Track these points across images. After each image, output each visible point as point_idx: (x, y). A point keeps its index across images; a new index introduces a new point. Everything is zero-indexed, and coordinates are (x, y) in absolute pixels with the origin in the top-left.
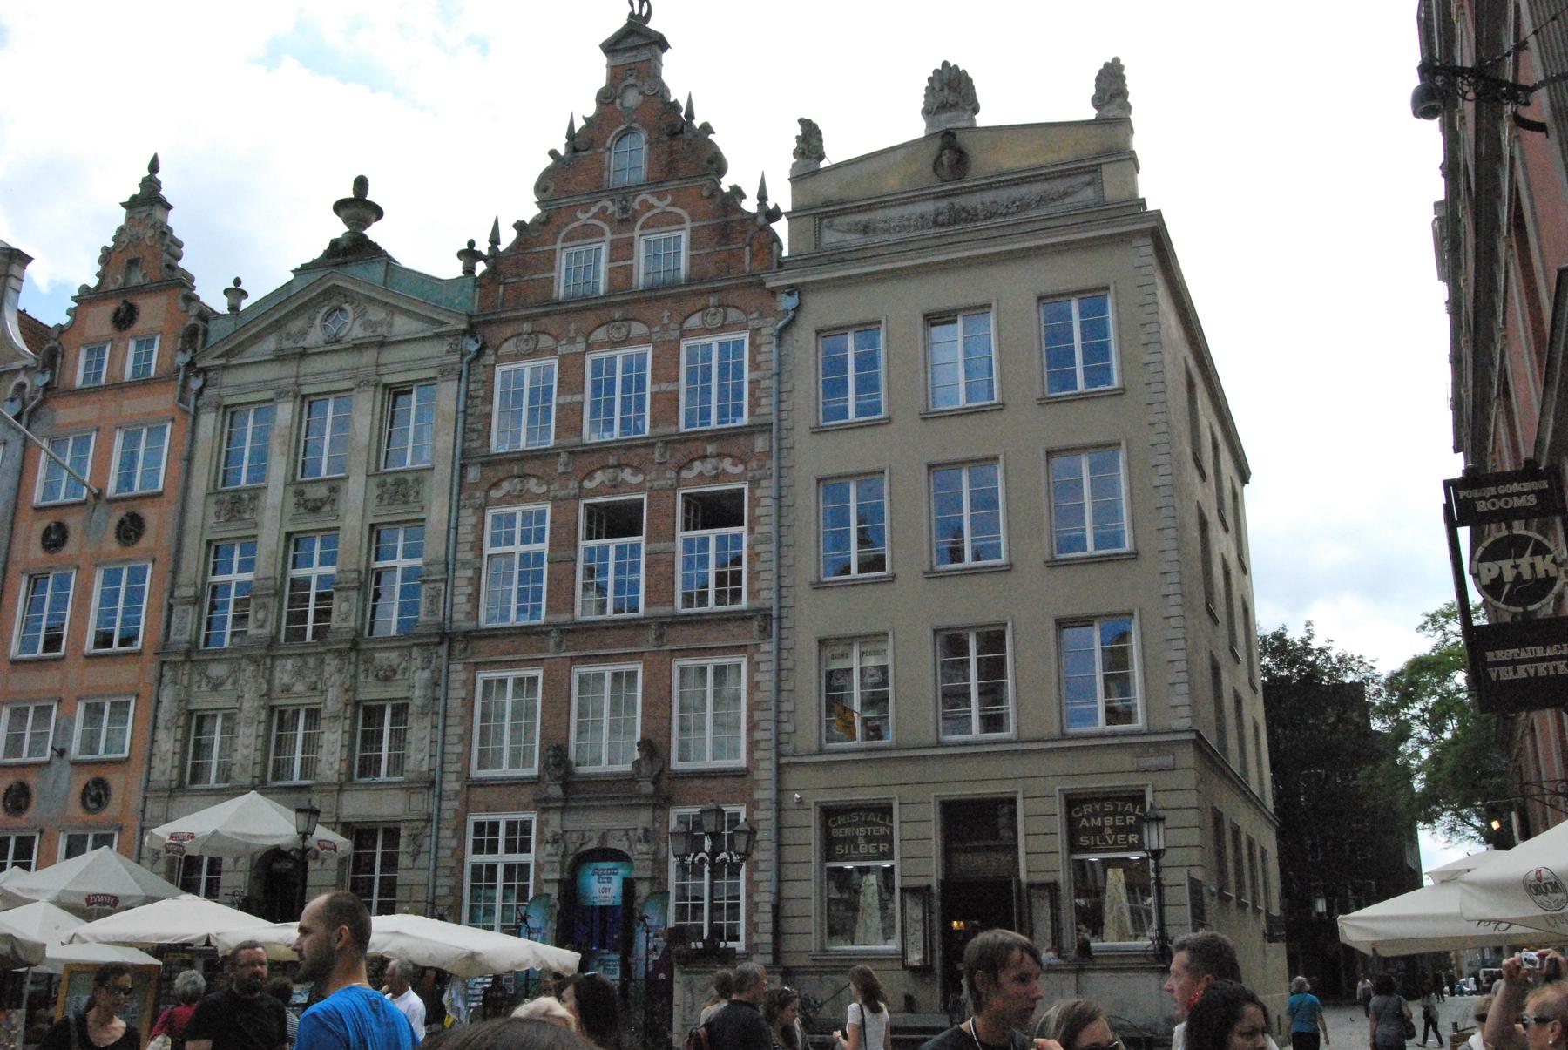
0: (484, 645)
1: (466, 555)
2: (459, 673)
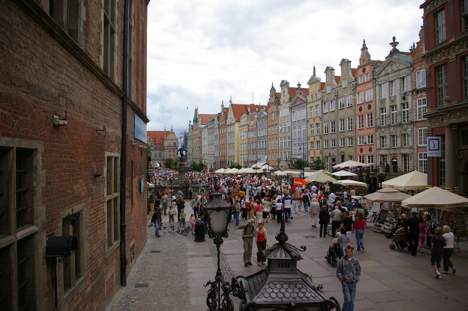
0: (418, 124)
1: (414, 108)
2: (415, 129)
